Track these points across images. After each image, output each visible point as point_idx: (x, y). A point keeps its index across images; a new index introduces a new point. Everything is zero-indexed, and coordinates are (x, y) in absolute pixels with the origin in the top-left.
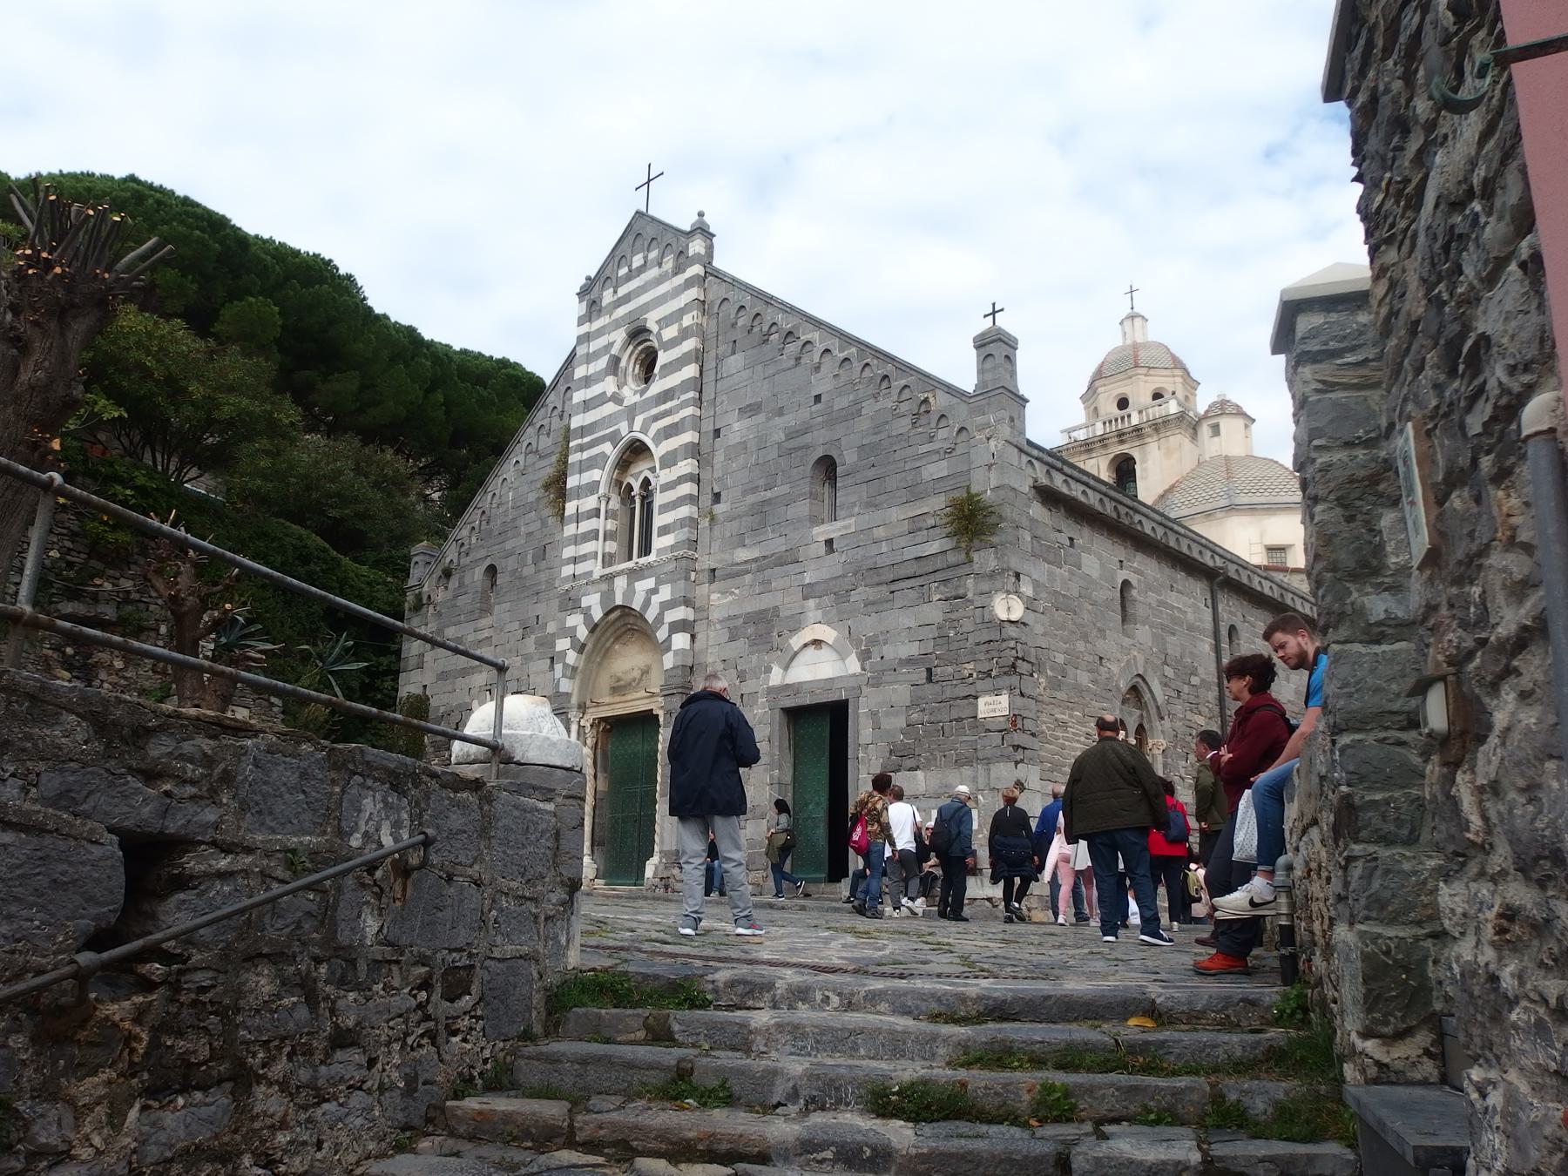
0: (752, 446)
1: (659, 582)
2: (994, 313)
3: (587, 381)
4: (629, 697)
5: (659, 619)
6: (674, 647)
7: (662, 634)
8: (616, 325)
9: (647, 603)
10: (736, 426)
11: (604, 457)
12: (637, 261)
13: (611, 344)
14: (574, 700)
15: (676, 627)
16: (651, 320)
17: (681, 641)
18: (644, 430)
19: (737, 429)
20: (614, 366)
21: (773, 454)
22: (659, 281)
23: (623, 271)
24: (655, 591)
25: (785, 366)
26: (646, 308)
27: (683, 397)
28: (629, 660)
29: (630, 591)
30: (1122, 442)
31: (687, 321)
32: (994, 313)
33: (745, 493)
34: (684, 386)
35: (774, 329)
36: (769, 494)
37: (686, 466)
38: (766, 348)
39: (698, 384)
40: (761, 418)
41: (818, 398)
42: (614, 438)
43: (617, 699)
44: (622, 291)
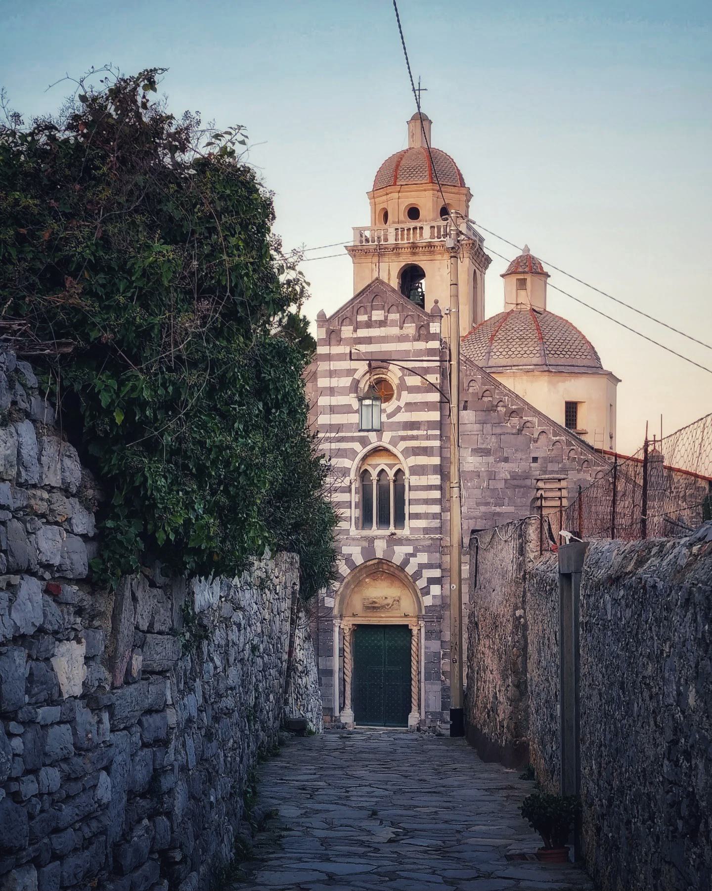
0: (484, 475)
1: (417, 550)
4: (378, 615)
5: (417, 575)
6: (432, 593)
7: (421, 583)
9: (406, 562)
10: (470, 459)
11: (354, 453)
13: (356, 370)
14: (336, 612)
15: (432, 581)
17: (435, 590)
18: (394, 442)
19: (471, 462)
20: (355, 387)
21: (501, 485)
24: (413, 555)
25: (509, 431)
27: (430, 432)
28: (380, 591)
29: (390, 551)
30: (414, 254)
33: (478, 504)
34: (431, 425)
35: (501, 403)
36: (498, 509)
37: (435, 480)
39: (440, 425)
40: (491, 459)
41: (535, 459)
42: (364, 442)
43: (370, 615)
44: (362, 333)
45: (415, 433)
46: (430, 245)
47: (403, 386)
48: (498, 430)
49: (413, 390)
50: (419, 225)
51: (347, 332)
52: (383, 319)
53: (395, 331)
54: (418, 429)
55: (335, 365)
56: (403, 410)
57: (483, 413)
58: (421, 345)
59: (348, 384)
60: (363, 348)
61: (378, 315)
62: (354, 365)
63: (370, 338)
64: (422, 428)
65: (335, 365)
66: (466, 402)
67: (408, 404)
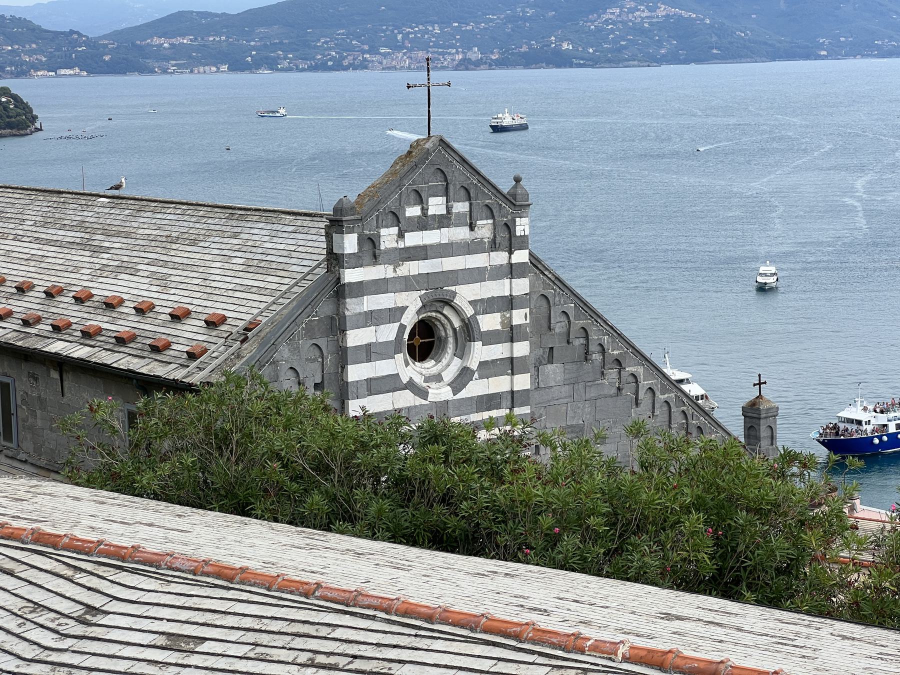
2: (760, 384)
3: (369, 353)
8: (408, 284)
13: (403, 309)
22: (470, 248)
23: (413, 211)
25: (606, 392)
31: (519, 317)
32: (760, 384)
38: (587, 366)
44: (413, 239)
45: (494, 413)
47: (469, 332)
48: (592, 393)
49: (490, 338)
51: (388, 237)
52: (445, 212)
53: (461, 233)
54: (498, 407)
56: (476, 375)
57: (574, 366)
58: (500, 258)
59: (392, 337)
61: (436, 206)
63: (425, 248)
64: (504, 404)
66: (552, 348)
67: (482, 364)
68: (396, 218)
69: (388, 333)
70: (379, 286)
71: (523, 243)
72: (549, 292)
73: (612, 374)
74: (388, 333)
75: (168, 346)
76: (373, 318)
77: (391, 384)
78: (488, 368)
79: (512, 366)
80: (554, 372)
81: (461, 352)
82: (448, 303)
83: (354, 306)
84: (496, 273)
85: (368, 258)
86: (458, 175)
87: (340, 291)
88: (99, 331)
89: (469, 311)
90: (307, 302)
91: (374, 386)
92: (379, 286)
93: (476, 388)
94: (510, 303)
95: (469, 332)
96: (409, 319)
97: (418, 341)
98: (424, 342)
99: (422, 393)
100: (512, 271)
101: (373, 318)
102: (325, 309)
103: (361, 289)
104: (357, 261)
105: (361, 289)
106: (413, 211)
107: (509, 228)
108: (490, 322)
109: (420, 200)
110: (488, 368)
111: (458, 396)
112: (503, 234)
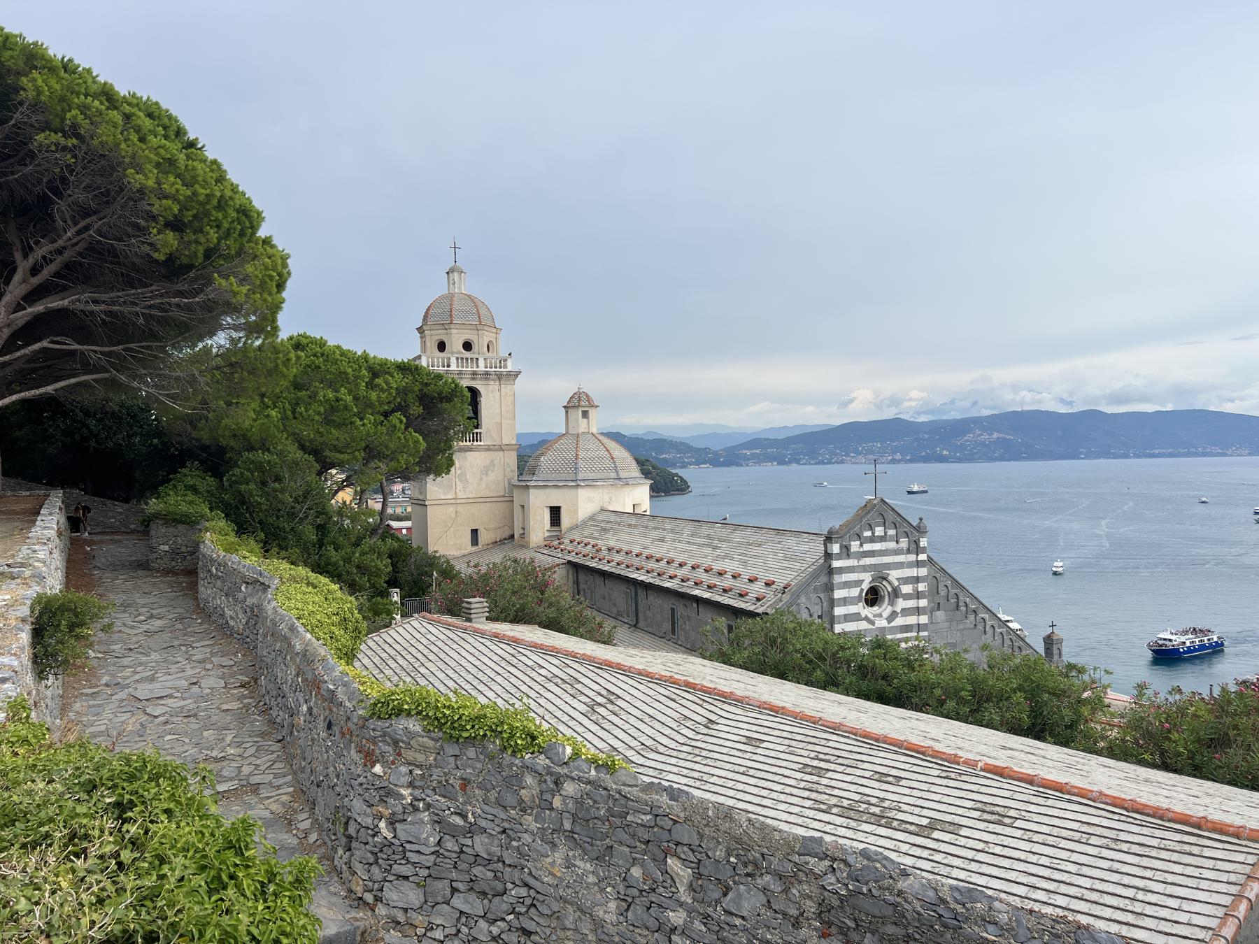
3: (845, 601)
8: (865, 569)
12: (879, 531)
16: (894, 575)
22: (897, 552)
23: (868, 534)
26: (889, 566)
31: (922, 587)
44: (867, 547)
45: (909, 635)
46: (487, 374)
47: (896, 593)
48: (961, 627)
49: (907, 597)
50: (475, 356)
51: (855, 546)
53: (892, 545)
55: (846, 577)
58: (912, 557)
60: (868, 561)
61: (879, 531)
62: (862, 576)
65: (846, 577)
68: (859, 537)
69: (855, 592)
70: (851, 570)
71: (924, 550)
72: (938, 575)
73: (972, 617)
74: (855, 592)
75: (747, 594)
76: (847, 585)
77: (856, 617)
78: (906, 612)
79: (918, 611)
80: (940, 615)
81: (892, 603)
82: (885, 579)
83: (837, 579)
84: (910, 565)
85: (844, 555)
86: (890, 516)
87: (831, 572)
88: (715, 586)
89: (896, 583)
90: (814, 576)
91: (848, 618)
92: (851, 570)
93: (899, 621)
94: (917, 580)
95: (896, 593)
96: (866, 586)
97: (870, 597)
98: (873, 598)
99: (872, 623)
100: (918, 564)
101: (847, 585)
102: (823, 579)
103: (841, 570)
104: (839, 557)
105: (841, 570)
106: (868, 534)
107: (917, 543)
108: (907, 589)
109: (871, 528)
110: (906, 612)
111: (893, 624)
112: (913, 546)
